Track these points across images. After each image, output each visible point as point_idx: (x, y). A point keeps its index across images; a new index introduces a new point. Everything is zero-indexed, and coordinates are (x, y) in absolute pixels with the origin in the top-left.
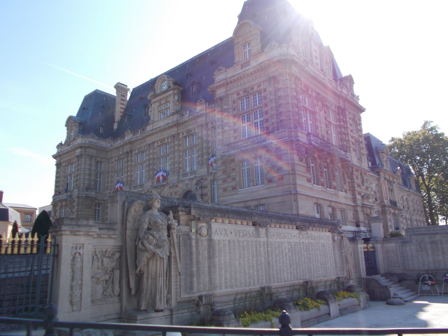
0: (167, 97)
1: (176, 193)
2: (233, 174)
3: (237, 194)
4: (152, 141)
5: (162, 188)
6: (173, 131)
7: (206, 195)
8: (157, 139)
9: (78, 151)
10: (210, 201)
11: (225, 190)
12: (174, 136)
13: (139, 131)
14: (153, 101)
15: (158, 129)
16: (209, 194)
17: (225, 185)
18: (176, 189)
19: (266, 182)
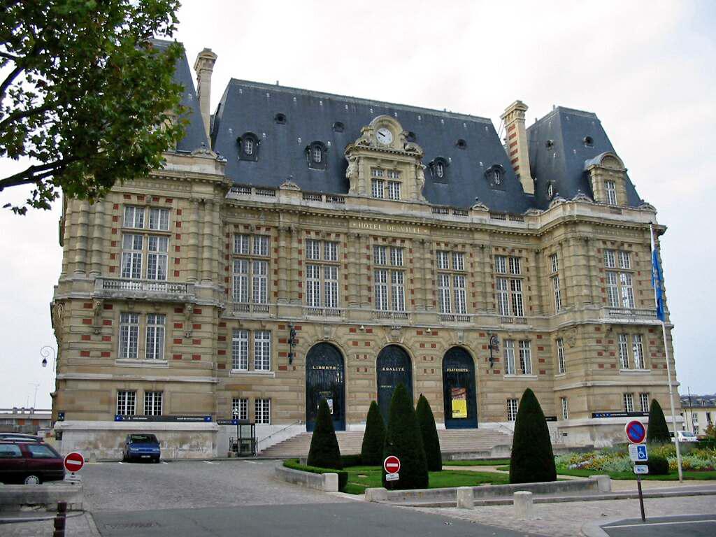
0: (399, 163)
1: (433, 346)
2: (612, 348)
3: (619, 375)
4: (366, 232)
5: (402, 330)
6: (422, 234)
7: (497, 360)
8: (379, 233)
9: (205, 192)
10: (503, 371)
11: (601, 366)
12: (423, 242)
13: (324, 198)
14: (363, 153)
15: (393, 219)
16: (502, 359)
17: (600, 360)
18: (434, 339)
19: (651, 366)
